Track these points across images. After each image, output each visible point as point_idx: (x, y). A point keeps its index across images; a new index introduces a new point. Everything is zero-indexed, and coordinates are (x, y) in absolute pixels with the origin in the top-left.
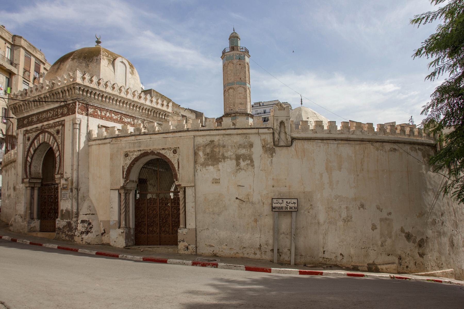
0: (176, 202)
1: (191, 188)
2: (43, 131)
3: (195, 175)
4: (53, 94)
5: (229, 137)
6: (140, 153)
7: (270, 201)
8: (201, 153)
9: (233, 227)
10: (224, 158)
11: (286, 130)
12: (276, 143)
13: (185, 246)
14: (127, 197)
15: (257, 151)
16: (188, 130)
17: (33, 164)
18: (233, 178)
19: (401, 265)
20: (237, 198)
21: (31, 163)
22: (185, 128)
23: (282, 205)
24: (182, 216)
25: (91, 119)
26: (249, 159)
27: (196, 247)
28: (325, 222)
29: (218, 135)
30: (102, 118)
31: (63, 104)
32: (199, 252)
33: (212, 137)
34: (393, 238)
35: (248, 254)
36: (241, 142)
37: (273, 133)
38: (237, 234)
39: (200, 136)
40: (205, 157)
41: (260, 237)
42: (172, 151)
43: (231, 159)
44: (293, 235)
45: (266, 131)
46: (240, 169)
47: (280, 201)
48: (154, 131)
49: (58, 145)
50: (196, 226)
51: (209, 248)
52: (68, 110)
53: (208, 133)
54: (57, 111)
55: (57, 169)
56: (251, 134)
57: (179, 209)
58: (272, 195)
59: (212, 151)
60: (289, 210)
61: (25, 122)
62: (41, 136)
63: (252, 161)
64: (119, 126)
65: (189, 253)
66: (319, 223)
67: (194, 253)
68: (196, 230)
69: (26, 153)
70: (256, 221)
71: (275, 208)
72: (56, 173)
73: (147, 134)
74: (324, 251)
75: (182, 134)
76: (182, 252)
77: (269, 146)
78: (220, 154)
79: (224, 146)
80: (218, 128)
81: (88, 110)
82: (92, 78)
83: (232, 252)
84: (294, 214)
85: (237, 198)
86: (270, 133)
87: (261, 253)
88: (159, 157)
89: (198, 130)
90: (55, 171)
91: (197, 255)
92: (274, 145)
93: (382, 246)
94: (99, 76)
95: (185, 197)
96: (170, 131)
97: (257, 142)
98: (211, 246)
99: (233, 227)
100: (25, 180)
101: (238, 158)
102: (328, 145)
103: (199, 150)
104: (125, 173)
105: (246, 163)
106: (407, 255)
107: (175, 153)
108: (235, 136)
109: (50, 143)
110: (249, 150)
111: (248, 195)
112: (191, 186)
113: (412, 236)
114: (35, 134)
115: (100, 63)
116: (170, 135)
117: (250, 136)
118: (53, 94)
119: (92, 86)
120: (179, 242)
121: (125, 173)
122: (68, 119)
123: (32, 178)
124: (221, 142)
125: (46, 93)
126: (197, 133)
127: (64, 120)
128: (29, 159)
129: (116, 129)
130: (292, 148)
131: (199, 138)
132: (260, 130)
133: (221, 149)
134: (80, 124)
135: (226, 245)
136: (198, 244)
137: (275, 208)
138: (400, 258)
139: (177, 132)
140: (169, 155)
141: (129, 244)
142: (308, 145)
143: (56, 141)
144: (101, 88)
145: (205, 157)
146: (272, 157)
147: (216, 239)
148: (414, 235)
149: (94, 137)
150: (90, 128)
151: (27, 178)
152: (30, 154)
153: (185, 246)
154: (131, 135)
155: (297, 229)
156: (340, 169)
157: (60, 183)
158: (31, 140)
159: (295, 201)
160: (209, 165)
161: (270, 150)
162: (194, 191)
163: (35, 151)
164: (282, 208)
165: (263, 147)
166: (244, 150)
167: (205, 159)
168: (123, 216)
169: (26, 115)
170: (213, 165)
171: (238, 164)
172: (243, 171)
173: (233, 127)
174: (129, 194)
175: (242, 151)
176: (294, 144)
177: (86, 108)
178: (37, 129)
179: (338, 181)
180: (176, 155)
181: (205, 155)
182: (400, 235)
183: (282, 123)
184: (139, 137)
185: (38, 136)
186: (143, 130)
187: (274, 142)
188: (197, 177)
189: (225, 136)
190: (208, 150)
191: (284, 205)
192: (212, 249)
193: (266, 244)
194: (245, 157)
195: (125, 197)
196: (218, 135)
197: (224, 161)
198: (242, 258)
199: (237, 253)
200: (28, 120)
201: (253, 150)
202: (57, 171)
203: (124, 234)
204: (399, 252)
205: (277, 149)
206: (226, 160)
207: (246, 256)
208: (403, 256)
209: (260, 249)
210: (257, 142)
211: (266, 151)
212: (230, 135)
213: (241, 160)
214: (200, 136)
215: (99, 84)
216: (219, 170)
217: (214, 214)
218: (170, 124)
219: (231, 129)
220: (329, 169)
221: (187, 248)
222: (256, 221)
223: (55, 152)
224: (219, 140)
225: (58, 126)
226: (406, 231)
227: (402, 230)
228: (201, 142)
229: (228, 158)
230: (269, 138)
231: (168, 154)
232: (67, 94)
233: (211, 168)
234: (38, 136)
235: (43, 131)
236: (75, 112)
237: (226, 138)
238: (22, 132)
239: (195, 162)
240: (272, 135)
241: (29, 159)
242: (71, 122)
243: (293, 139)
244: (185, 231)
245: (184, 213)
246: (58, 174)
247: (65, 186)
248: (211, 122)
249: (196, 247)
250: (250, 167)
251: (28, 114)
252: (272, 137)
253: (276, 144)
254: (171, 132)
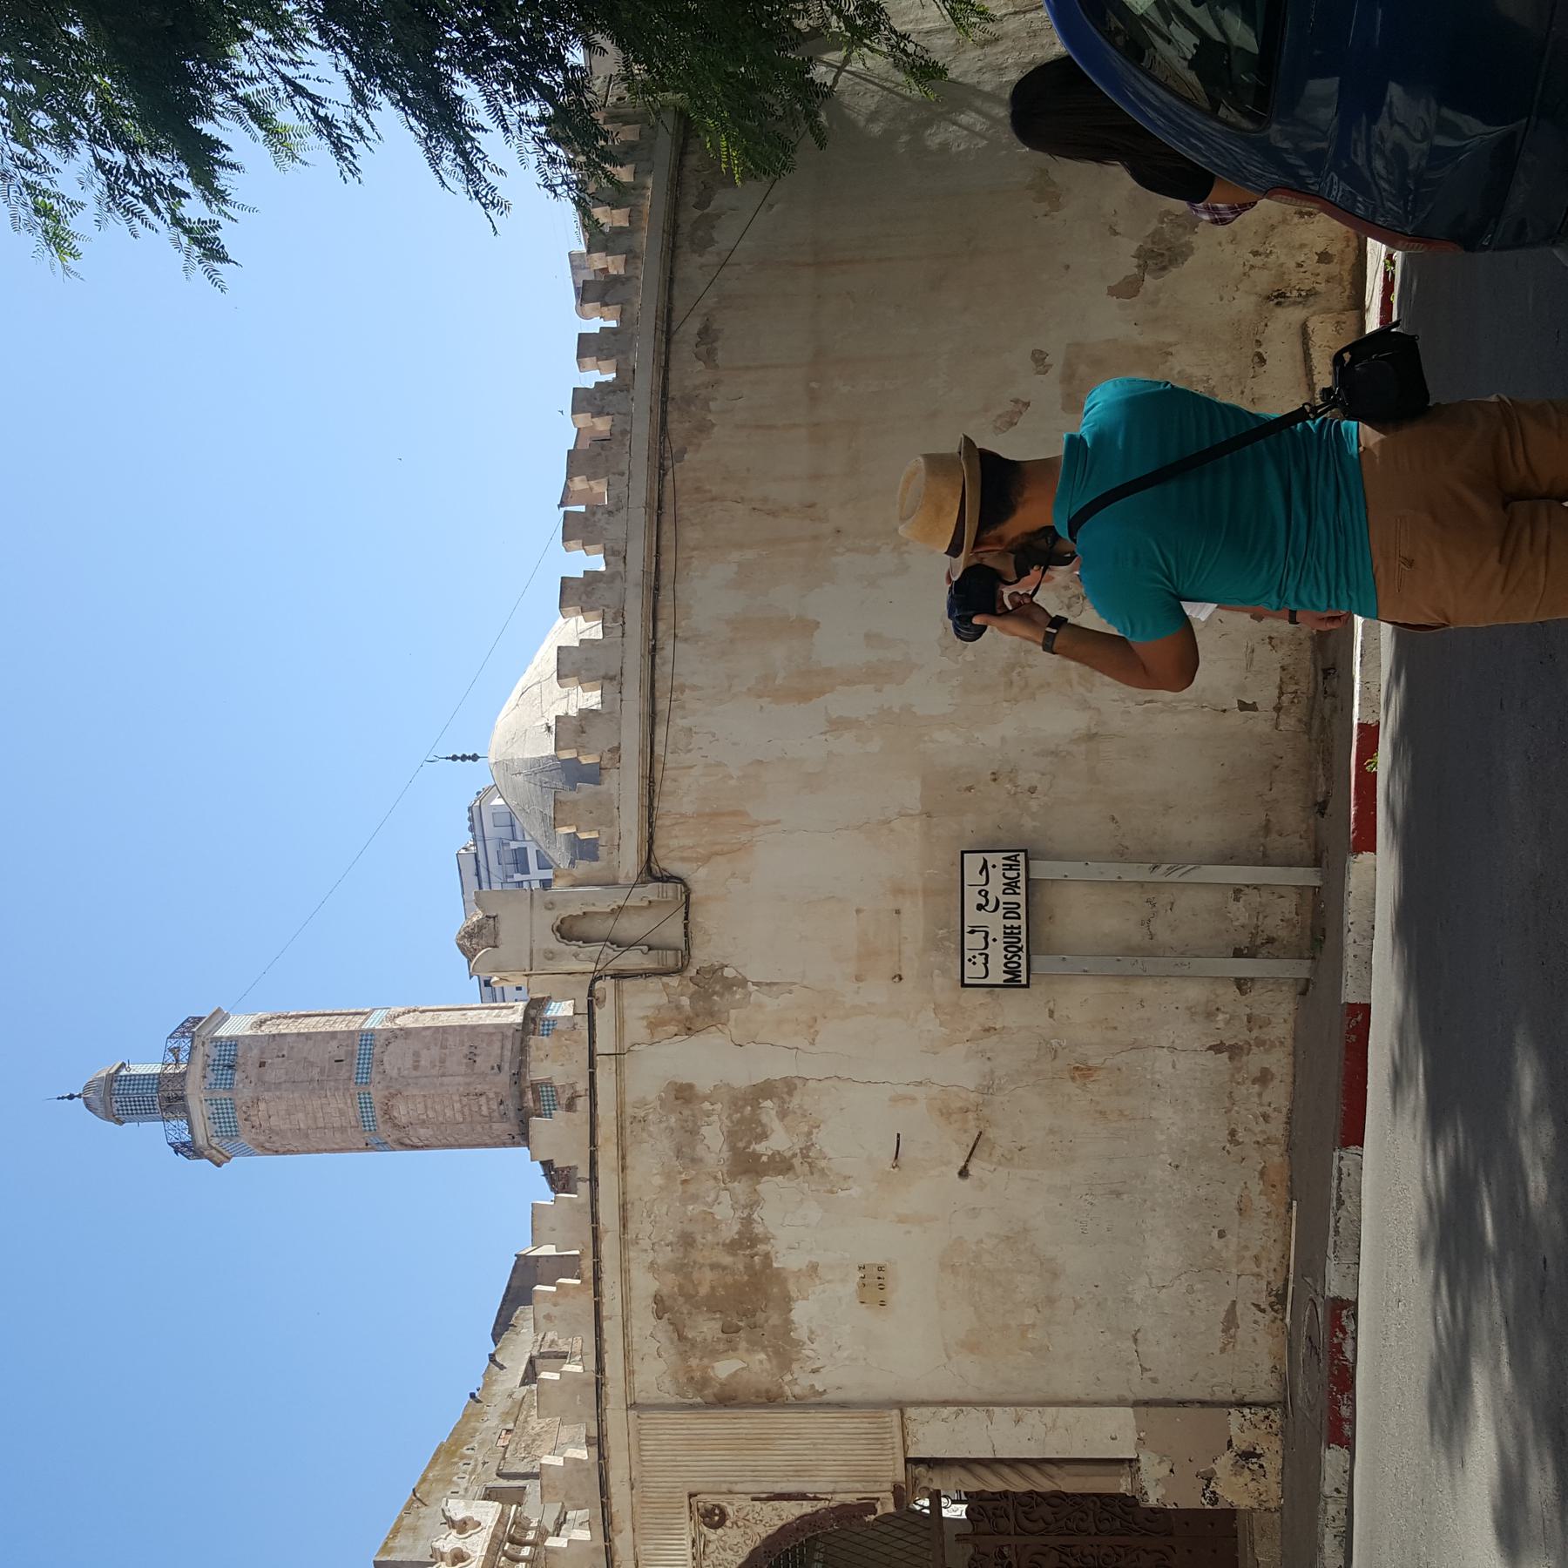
0: (989, 1506)
1: (911, 1426)
3: (843, 1405)
5: (635, 1215)
8: (723, 1369)
9: (1118, 1194)
10: (747, 1240)
11: (603, 907)
12: (670, 960)
13: (1237, 1470)
15: (709, 1061)
18: (856, 1191)
19: (1312, 293)
20: (964, 1173)
22: (582, 1454)
23: (997, 932)
24: (1070, 1484)
26: (756, 1106)
27: (1241, 1404)
29: (624, 1271)
32: (1264, 1386)
33: (634, 1305)
34: (1169, 337)
35: (1266, 1117)
36: (665, 1145)
37: (619, 976)
39: (629, 1373)
40: (743, 1345)
41: (1172, 1049)
42: (712, 1535)
43: (753, 1204)
44: (1158, 876)
45: (604, 1016)
46: (805, 1153)
47: (974, 942)
50: (1121, 1402)
51: (1244, 1332)
53: (611, 1329)
56: (620, 1092)
58: (944, 984)
59: (713, 1305)
60: (1021, 899)
63: (765, 1090)
65: (1276, 1445)
66: (1091, 737)
67: (1276, 1415)
68: (1147, 1403)
70: (1083, 1072)
76: (1271, 1486)
77: (685, 1001)
78: (727, 1260)
79: (687, 1241)
80: (589, 1274)
83: (1260, 1203)
84: (1041, 870)
85: (964, 1173)
86: (617, 988)
87: (1260, 1043)
89: (599, 1385)
91: (1283, 1404)
92: (679, 971)
95: (966, 1464)
96: (601, 1543)
98: (1230, 1321)
99: (1118, 1194)
101: (748, 1166)
102: (682, 688)
103: (706, 1381)
105: (776, 1125)
106: (1258, 261)
107: (723, 1516)
108: (633, 1178)
110: (707, 1106)
111: (946, 1113)
112: (903, 1426)
113: (1156, 236)
116: (622, 1543)
117: (629, 1098)
120: (1215, 1499)
124: (666, 1256)
126: (614, 1389)
130: (698, 876)
131: (638, 1380)
132: (600, 1047)
133: (696, 1255)
135: (1221, 1234)
136: (1223, 1394)
138: (1279, 298)
139: (605, 1506)
142: (680, 799)
145: (743, 1345)
146: (743, 983)
147: (1190, 1290)
148: (1153, 225)
153: (1237, 1470)
155: (1121, 855)
156: (808, 627)
159: (973, 862)
160: (788, 1324)
161: (705, 994)
162: (927, 1412)
164: (1010, 933)
165: (689, 1031)
166: (705, 1130)
167: (754, 1345)
170: (786, 1302)
172: (820, 1137)
173: (584, 1187)
175: (714, 1141)
176: (676, 868)
179: (867, 636)
180: (730, 1510)
181: (732, 1347)
182: (1154, 303)
183: (566, 931)
187: (667, 974)
188: (854, 1394)
189: (630, 1236)
190: (707, 1328)
191: (996, 923)
192: (1246, 1315)
193: (1210, 1015)
194: (746, 1129)
196: (624, 1271)
197: (766, 1239)
198: (1290, 1148)
199: (1262, 1174)
201: (704, 1085)
204: (1244, 303)
205: (702, 956)
206: (758, 1229)
207: (1277, 1128)
208: (1263, 281)
211: (712, 1014)
212: (623, 1207)
213: (759, 1148)
214: (629, 1373)
216: (814, 1268)
217: (1051, 1301)
219: (594, 1200)
220: (808, 685)
221: (1248, 1455)
222: (1083, 1072)
224: (652, 1266)
226: (1129, 266)
227: (1128, 289)
228: (660, 1366)
229: (748, 1221)
230: (645, 998)
231: (729, 1555)
233: (802, 1313)
237: (640, 1226)
239: (771, 1400)
243: (651, 872)
244: (1148, 1462)
245: (1053, 1470)
248: (555, 1311)
249: (1241, 1404)
250: (795, 1102)
252: (640, 981)
253: (676, 961)
254: (607, 1538)
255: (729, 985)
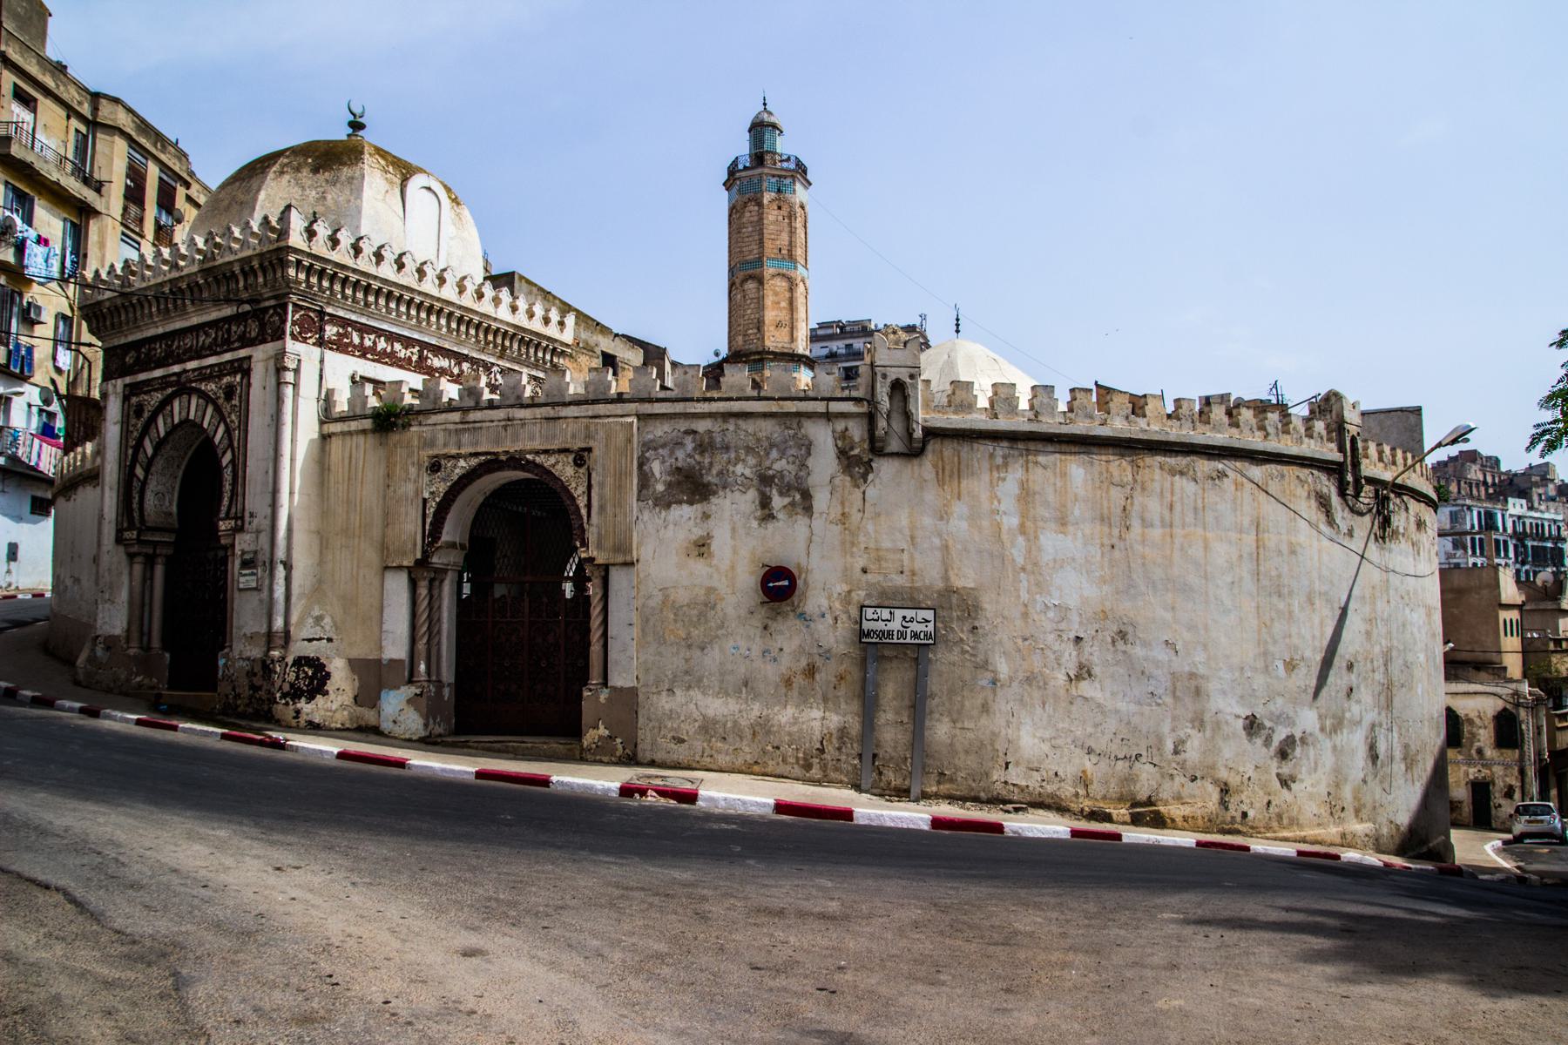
2: (182, 387)
4: (215, 278)
6: (474, 462)
7: (854, 612)
14: (436, 592)
16: (620, 399)
17: (152, 485)
21: (144, 483)
22: (613, 391)
25: (329, 354)
28: (1011, 679)
30: (363, 356)
31: (247, 307)
37: (871, 418)
38: (756, 709)
45: (848, 407)
47: (885, 614)
48: (519, 397)
49: (228, 431)
52: (262, 326)
53: (679, 408)
54: (229, 331)
55: (226, 502)
57: (588, 630)
58: (859, 595)
60: (908, 640)
61: (129, 360)
62: (176, 404)
63: (807, 495)
64: (415, 380)
69: (130, 451)
71: (868, 635)
72: (222, 515)
73: (498, 407)
74: (1007, 764)
75: (601, 409)
77: (856, 452)
80: (708, 395)
81: (322, 330)
82: (336, 231)
88: (530, 476)
90: (219, 511)
93: (1176, 752)
94: (358, 227)
96: (568, 399)
97: (822, 437)
100: (127, 535)
104: (429, 521)
109: (205, 425)
114: (159, 396)
115: (360, 190)
118: (215, 278)
119: (334, 256)
121: (429, 521)
122: (260, 355)
123: (150, 529)
125: (195, 274)
127: (250, 358)
128: (139, 472)
129: (405, 389)
134: (297, 371)
137: (868, 635)
140: (565, 470)
141: (439, 730)
143: (223, 419)
144: (365, 264)
148: (1268, 724)
149: (338, 409)
150: (329, 383)
151: (131, 527)
152: (141, 456)
154: (450, 407)
157: (233, 546)
158: (146, 415)
159: (929, 615)
160: (680, 502)
161: (857, 464)
163: (158, 447)
164: (890, 633)
167: (669, 485)
168: (421, 645)
169: (131, 338)
170: (691, 503)
171: (765, 503)
173: (755, 394)
174: (442, 581)
177: (313, 327)
178: (164, 382)
184: (473, 416)
185: (167, 401)
186: (487, 395)
191: (895, 625)
195: (430, 590)
200: (139, 352)
202: (224, 509)
203: (423, 701)
209: (822, 751)
210: (822, 437)
215: (357, 250)
218: (568, 379)
219: (748, 399)
223: (220, 452)
225: (229, 374)
230: (857, 431)
232: (261, 280)
234: (167, 401)
235: (182, 387)
236: (284, 333)
238: (120, 388)
240: (865, 421)
241: (139, 472)
242: (272, 362)
244: (604, 695)
246: (228, 517)
247: (247, 557)
251: (138, 336)
253: (877, 448)
255: (864, 477)
